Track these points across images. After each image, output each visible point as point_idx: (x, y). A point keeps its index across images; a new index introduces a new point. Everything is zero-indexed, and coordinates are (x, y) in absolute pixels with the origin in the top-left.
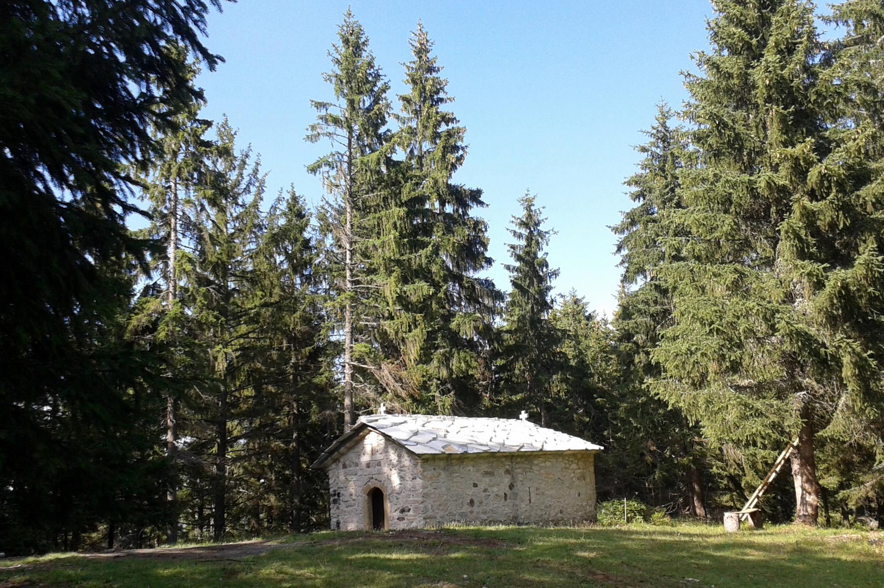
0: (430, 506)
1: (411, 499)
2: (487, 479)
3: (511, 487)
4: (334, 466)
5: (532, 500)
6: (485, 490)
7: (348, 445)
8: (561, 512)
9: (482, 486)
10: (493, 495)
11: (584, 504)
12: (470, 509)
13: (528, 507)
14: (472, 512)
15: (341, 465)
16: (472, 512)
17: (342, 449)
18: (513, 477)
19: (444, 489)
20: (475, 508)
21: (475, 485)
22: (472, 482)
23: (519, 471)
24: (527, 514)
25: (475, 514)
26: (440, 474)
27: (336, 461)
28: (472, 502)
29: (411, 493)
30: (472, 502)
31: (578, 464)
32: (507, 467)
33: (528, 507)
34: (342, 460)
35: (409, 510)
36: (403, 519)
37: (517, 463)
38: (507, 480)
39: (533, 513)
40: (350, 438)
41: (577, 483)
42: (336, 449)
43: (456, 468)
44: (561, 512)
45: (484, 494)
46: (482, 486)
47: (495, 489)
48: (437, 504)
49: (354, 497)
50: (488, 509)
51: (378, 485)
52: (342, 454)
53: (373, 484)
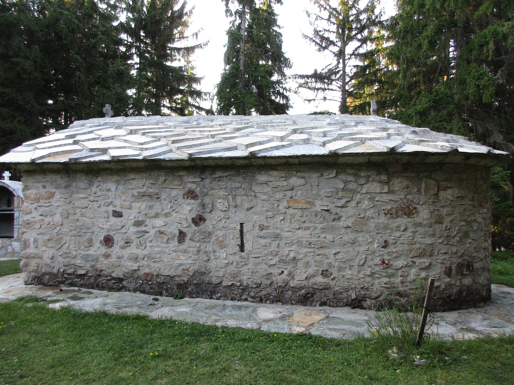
0: (32, 240)
2: (141, 205)
3: (198, 220)
5: (248, 246)
6: (138, 224)
8: (325, 273)
9: (130, 216)
10: (152, 232)
11: (400, 263)
12: (104, 250)
13: (237, 258)
14: (107, 256)
16: (107, 256)
18: (203, 206)
19: (58, 218)
20: (116, 250)
21: (118, 214)
22: (111, 208)
23: (222, 193)
24: (232, 268)
25: (113, 259)
26: (52, 195)
28: (108, 241)
30: (108, 241)
31: (387, 183)
32: (193, 186)
33: (237, 258)
37: (215, 179)
38: (188, 209)
39: (244, 269)
41: (383, 219)
43: (82, 185)
44: (325, 273)
45: (134, 229)
46: (130, 216)
47: (159, 222)
48: (47, 237)
50: (140, 252)
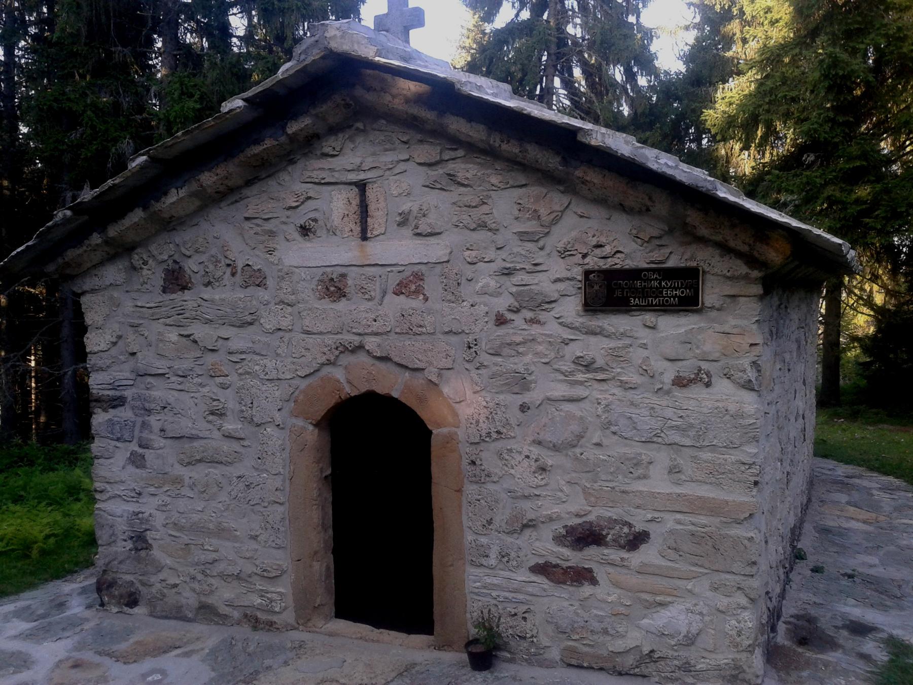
1: (659, 483)
4: (112, 273)
7: (208, 179)
15: (154, 275)
17: (174, 198)
27: (121, 250)
29: (662, 458)
34: (163, 250)
35: (637, 540)
36: (582, 576)
40: (229, 142)
42: (146, 191)
49: (230, 426)
51: (393, 384)
52: (168, 224)
53: (351, 378)
